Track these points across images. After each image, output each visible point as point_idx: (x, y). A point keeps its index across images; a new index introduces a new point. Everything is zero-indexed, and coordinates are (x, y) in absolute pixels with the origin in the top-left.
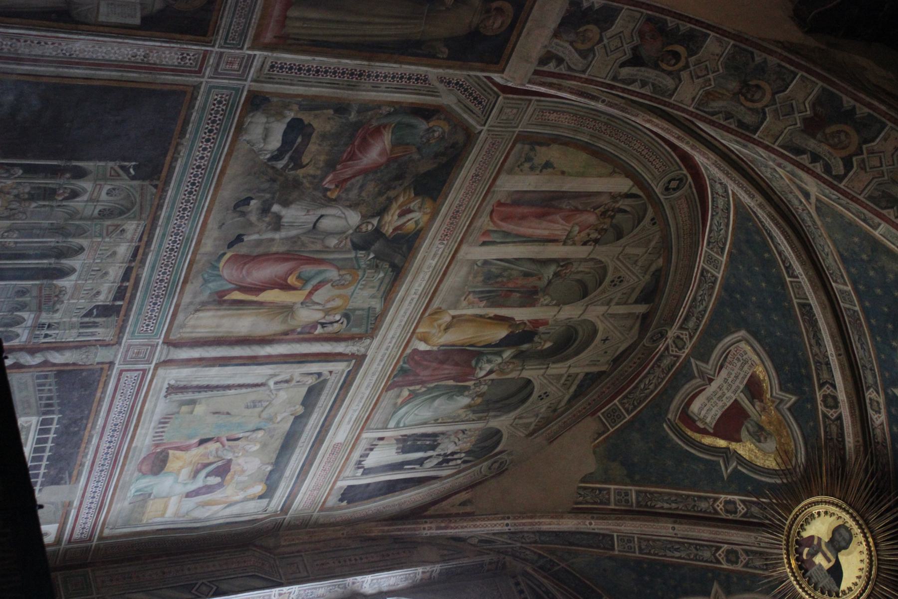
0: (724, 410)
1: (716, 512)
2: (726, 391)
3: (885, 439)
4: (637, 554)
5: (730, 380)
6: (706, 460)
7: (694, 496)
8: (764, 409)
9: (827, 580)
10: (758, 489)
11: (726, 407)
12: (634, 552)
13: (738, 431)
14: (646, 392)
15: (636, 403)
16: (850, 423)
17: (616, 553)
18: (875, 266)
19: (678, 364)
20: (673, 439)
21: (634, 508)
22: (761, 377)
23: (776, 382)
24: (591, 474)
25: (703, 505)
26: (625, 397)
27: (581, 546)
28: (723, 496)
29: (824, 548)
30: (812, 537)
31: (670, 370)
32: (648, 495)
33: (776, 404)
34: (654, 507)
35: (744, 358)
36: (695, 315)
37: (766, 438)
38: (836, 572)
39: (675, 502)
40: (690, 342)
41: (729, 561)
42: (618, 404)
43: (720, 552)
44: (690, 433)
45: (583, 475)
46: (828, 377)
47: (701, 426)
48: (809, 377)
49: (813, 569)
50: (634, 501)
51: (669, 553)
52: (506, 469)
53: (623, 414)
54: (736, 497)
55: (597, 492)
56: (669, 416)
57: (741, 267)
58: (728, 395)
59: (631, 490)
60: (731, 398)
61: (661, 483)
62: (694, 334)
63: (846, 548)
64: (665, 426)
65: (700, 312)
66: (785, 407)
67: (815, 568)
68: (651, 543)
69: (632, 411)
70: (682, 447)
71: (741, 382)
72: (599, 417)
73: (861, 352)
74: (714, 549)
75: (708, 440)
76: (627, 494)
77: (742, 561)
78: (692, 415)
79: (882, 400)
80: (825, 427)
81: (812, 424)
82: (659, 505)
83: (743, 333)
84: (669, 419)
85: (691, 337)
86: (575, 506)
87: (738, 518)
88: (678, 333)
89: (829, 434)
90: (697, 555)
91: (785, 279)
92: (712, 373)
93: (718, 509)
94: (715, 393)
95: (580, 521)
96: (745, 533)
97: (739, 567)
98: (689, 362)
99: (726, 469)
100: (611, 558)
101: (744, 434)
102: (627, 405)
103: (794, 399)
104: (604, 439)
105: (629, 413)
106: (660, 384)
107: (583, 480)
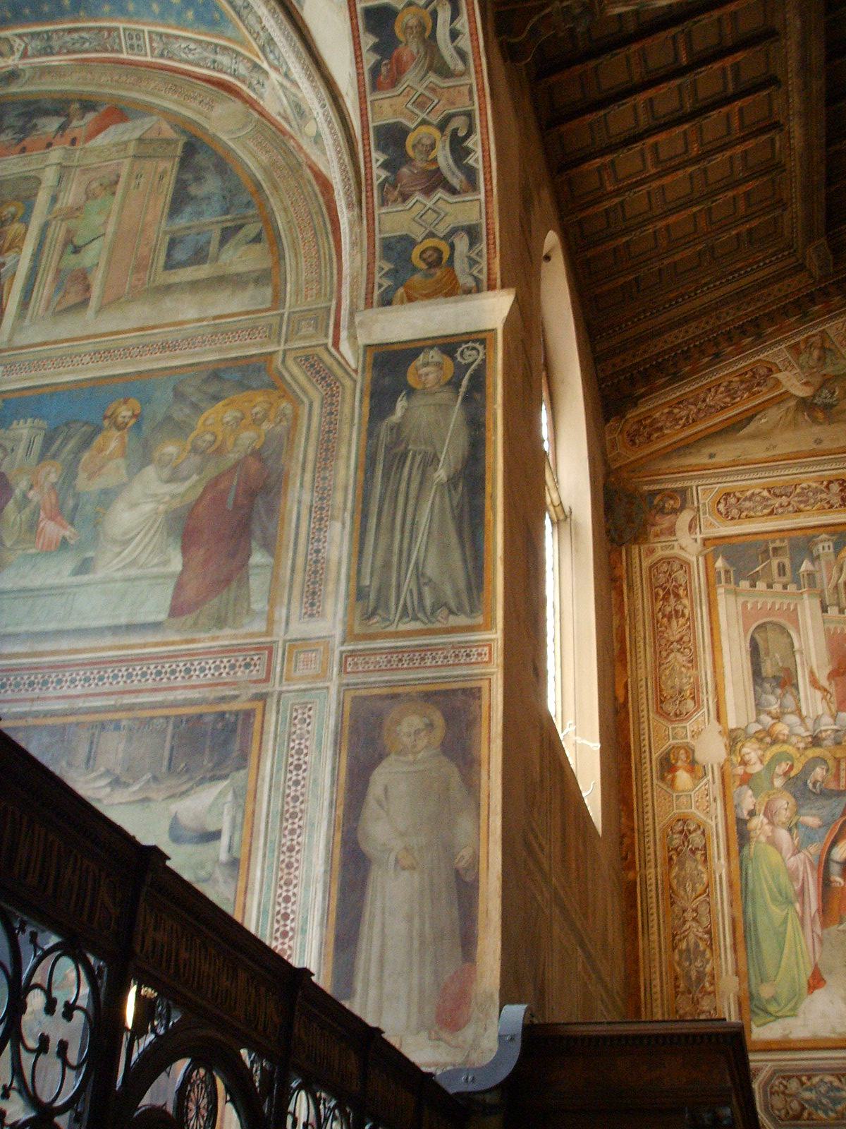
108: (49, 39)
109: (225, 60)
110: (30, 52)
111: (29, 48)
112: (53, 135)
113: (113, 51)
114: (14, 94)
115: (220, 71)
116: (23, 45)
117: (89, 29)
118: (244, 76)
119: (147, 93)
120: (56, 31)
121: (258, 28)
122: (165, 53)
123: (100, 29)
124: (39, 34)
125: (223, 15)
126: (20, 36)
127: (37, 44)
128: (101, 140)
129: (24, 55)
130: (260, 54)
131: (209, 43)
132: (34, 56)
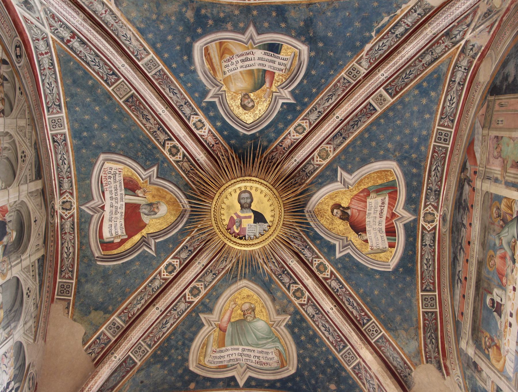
0: (123, 217)
1: (166, 279)
2: (116, 205)
3: (216, 138)
4: (150, 351)
5: (114, 195)
6: (137, 256)
7: (148, 284)
8: (144, 191)
10: (175, 241)
11: (123, 214)
12: (148, 351)
13: (140, 220)
14: (70, 256)
15: (70, 269)
16: (195, 146)
17: (139, 363)
18: (162, 19)
19: (76, 220)
20: (110, 265)
21: (125, 327)
22: (130, 174)
23: (140, 168)
24: (85, 334)
25: (157, 283)
26: (61, 272)
27: (119, 382)
28: (162, 267)
29: (242, 215)
30: (232, 218)
31: (73, 229)
32: (125, 311)
33: (148, 183)
34: (134, 314)
35: (112, 173)
36: (65, 177)
37: (158, 208)
38: (259, 218)
39: (142, 298)
40: (73, 197)
41: (195, 296)
42: (60, 280)
43: (187, 297)
44: (115, 252)
45: (81, 341)
46: (164, 137)
47: (117, 240)
48: (155, 147)
50: (121, 323)
51: (165, 330)
52: (37, 383)
53: (68, 283)
54: (169, 260)
55: (98, 340)
56: (96, 255)
57: (77, 109)
58: (119, 205)
59: (114, 319)
61: (125, 296)
62: (72, 189)
63: (252, 201)
64: (99, 263)
65: (67, 171)
66: (154, 179)
67: (247, 229)
68: (151, 335)
69: (72, 275)
70: (119, 264)
71: (121, 190)
72: (57, 299)
73: (174, 98)
74: (183, 299)
75: (128, 245)
76: (114, 324)
78: (108, 240)
79: (201, 116)
80: (181, 168)
81: (174, 174)
82: (135, 309)
83: (102, 157)
84: (97, 257)
85: (72, 194)
86: (95, 362)
88: (62, 200)
89: (185, 170)
90: (178, 312)
91: (108, 90)
92: (100, 202)
93: (165, 276)
94: (111, 212)
95: (108, 363)
97: (203, 292)
98: (82, 210)
99: (151, 249)
100: (140, 370)
101: (145, 219)
102: (67, 276)
103: (155, 169)
104: (73, 308)
105: (71, 278)
106: (74, 243)
107: (84, 344)
108: (431, 189)
109: (459, 76)
110: (436, 205)
111: (433, 203)
112: (470, 188)
113: (445, 153)
114: (451, 216)
115: (465, 80)
116: (430, 206)
117: (431, 164)
118: (468, 63)
119: (466, 128)
120: (427, 186)
121: (443, 46)
122: (451, 118)
123: (433, 157)
124: (427, 194)
125: (435, 72)
126: (426, 206)
127: (432, 198)
128: (478, 155)
129: (436, 208)
130: (457, 46)
131: (449, 84)
132: (438, 205)
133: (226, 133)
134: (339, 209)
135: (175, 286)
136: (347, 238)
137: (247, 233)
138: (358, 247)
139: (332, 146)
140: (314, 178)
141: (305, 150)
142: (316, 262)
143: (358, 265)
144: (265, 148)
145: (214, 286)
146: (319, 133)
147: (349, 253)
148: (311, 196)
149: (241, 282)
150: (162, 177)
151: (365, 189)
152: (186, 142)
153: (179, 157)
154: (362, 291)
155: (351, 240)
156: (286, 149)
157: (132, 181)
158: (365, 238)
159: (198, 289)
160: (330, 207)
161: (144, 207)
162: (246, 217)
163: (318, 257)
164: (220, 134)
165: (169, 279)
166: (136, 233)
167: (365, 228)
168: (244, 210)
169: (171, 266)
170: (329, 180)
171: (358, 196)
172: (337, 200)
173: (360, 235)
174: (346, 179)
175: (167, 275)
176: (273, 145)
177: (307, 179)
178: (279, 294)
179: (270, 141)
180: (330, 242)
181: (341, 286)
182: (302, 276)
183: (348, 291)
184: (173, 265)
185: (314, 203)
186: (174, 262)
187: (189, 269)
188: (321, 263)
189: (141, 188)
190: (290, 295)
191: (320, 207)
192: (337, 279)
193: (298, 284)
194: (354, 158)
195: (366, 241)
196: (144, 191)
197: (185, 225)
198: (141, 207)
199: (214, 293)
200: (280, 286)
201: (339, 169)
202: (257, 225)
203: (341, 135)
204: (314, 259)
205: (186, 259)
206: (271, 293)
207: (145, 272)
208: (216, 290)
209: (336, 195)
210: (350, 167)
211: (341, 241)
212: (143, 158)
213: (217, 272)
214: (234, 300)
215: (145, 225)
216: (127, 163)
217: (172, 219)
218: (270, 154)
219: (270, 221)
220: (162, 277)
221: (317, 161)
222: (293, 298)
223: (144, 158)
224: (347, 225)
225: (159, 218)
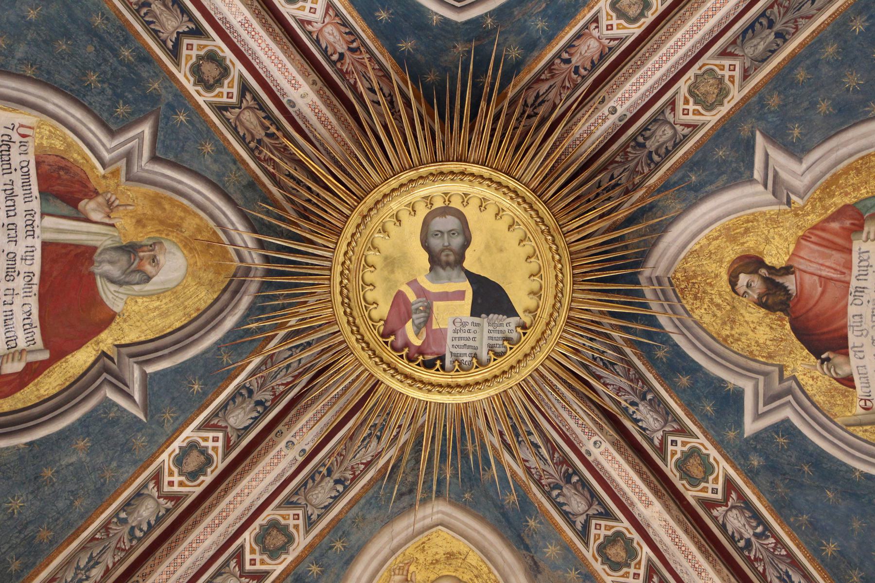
0: (35, 288)
1: (176, 498)
3: (352, 32)
6: (82, 421)
7: (116, 514)
8: (109, 204)
9: (486, 327)
11: (36, 280)
13: (94, 299)
16: (282, 56)
22: (59, 145)
23: (93, 127)
25: (146, 511)
28: (164, 456)
29: (433, 288)
30: (399, 298)
33: (123, 179)
37: (154, 260)
39: (93, 562)
41: (274, 553)
43: (248, 556)
48: (147, 58)
49: (449, 342)
54: (189, 433)
58: (20, 250)
60: (31, 249)
66: (144, 165)
67: (450, 334)
70: (16, 448)
71: (28, 198)
74: (233, 564)
77: (296, 527)
80: (234, 131)
81: (209, 148)
87: (221, 466)
93: (176, 488)
96: (267, 459)
97: (302, 542)
99: (129, 397)
103: (146, 129)
133: (383, 15)
134: (755, 272)
135: (208, 520)
136: (782, 369)
137: (449, 349)
138: (819, 399)
139: (737, 63)
140: (674, 169)
141: (645, 77)
142: (678, 448)
143: (818, 459)
144: (513, 70)
145: (337, 520)
146: (694, 20)
147: (787, 420)
148: (662, 229)
149: (428, 510)
150: (171, 157)
151: (846, 206)
152: (252, 43)
153: (228, 91)
154: (831, 548)
155: (794, 378)
156: (583, 72)
157: (66, 169)
158: (843, 371)
159: (283, 530)
160: (726, 265)
161: (107, 256)
162: (445, 296)
163: (683, 431)
164: (365, 19)
165: (187, 496)
166: (78, 345)
167: (845, 338)
168: (441, 271)
169: (195, 453)
170: (724, 177)
171: (823, 230)
172: (751, 243)
173: (828, 359)
174: (783, 175)
175: (181, 484)
176: (539, 58)
177: (652, 173)
178: (552, 551)
179: (532, 46)
180: (723, 381)
181: (760, 529)
182: (630, 494)
183: (785, 546)
184: (203, 451)
185: (673, 250)
186: (206, 439)
187: (254, 464)
188: (694, 452)
189: (97, 193)
190: (589, 554)
191: (692, 265)
192: (746, 505)
193: (616, 519)
194: (813, 105)
195: (848, 381)
196: (109, 204)
197: (245, 319)
198: (96, 257)
199: (339, 545)
200: (556, 525)
201: (760, 140)
202: (484, 321)
203: (771, 24)
204: (670, 438)
205: (247, 429)
206: (527, 548)
207: (108, 475)
208: (346, 534)
209: (748, 225)
210: (796, 132)
211: (761, 378)
212: (103, 91)
213: (349, 475)
214: (403, 569)
215: (109, 319)
216: (50, 107)
217: (203, 297)
218: (529, 86)
219: (527, 311)
220: (166, 488)
221: (686, 112)
222: (598, 566)
223: (109, 92)
224: (783, 327)
225: (158, 295)
